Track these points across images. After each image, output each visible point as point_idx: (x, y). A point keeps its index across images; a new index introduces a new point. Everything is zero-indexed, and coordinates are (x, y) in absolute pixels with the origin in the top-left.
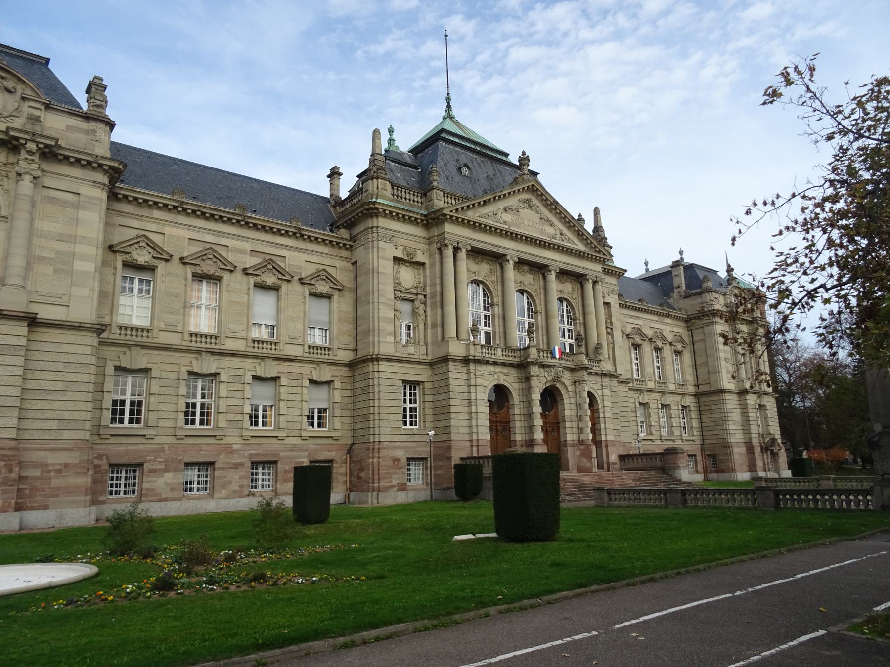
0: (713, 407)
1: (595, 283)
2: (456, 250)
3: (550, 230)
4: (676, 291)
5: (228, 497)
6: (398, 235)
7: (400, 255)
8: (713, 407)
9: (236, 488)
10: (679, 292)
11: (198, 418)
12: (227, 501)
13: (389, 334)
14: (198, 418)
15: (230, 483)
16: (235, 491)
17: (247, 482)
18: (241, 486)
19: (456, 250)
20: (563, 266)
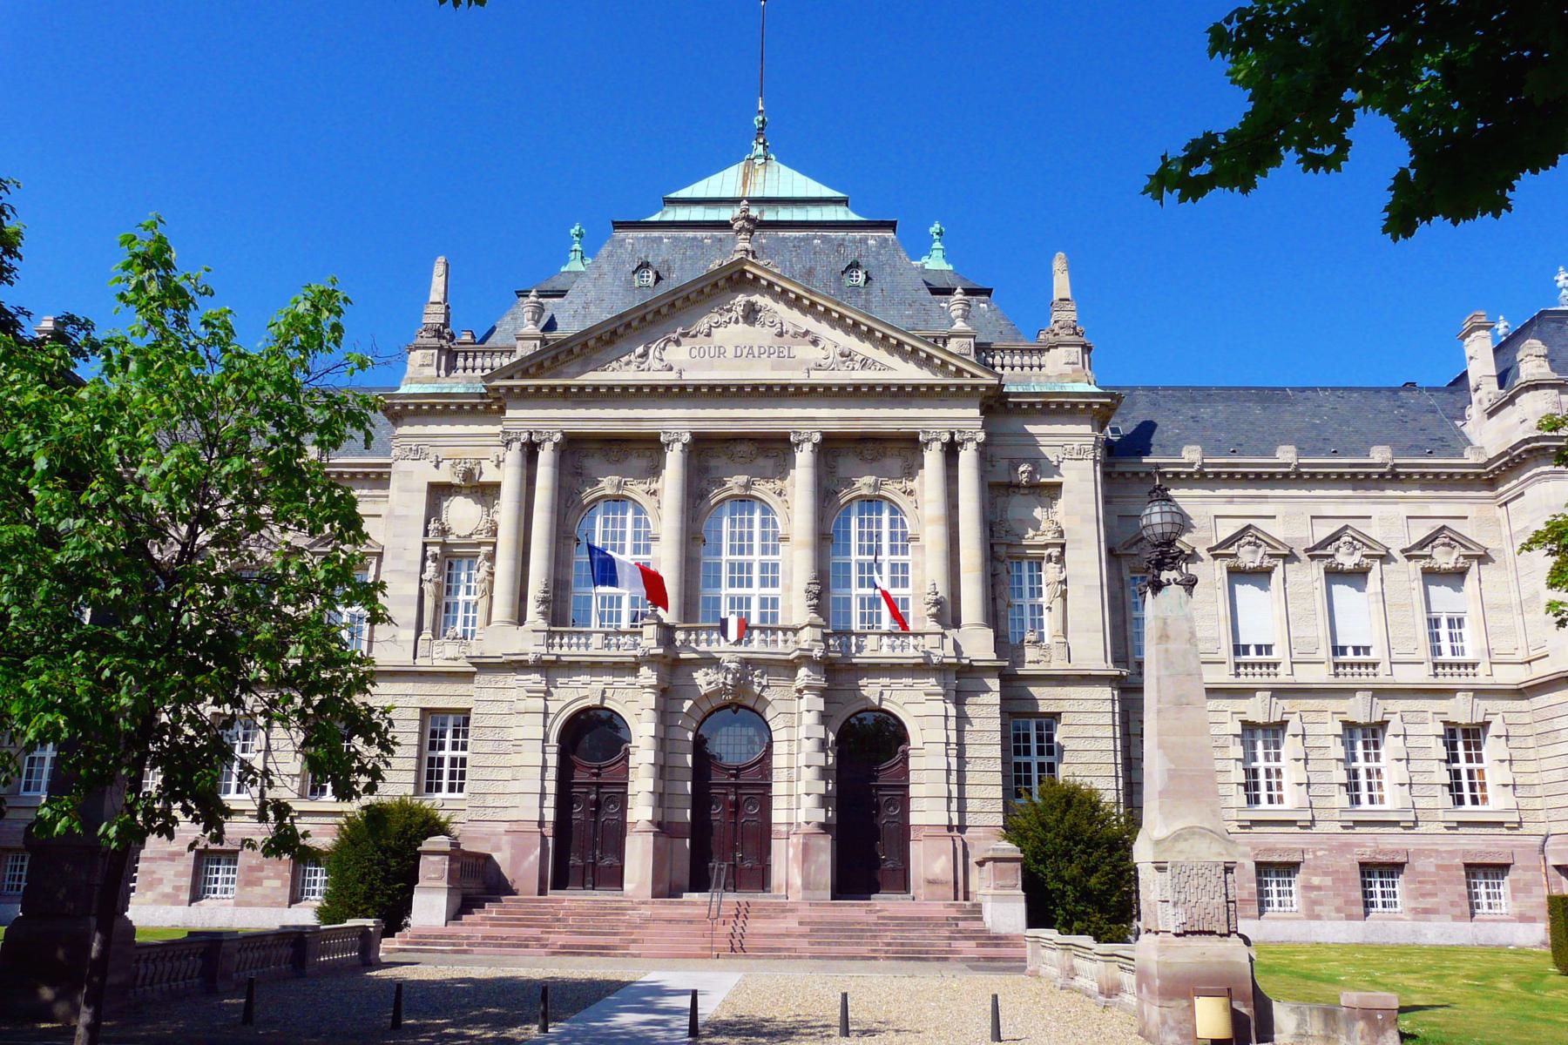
0: (1557, 724)
1: (951, 451)
2: (530, 451)
3: (815, 354)
4: (1475, 398)
5: (155, 901)
6: (439, 441)
7: (445, 475)
8: (1557, 724)
9: (168, 889)
10: (1480, 401)
11: (445, 781)
12: (151, 909)
13: (406, 626)
14: (445, 781)
15: (160, 881)
16: (166, 896)
17: (186, 882)
18: (177, 888)
19: (530, 451)
20: (834, 427)
